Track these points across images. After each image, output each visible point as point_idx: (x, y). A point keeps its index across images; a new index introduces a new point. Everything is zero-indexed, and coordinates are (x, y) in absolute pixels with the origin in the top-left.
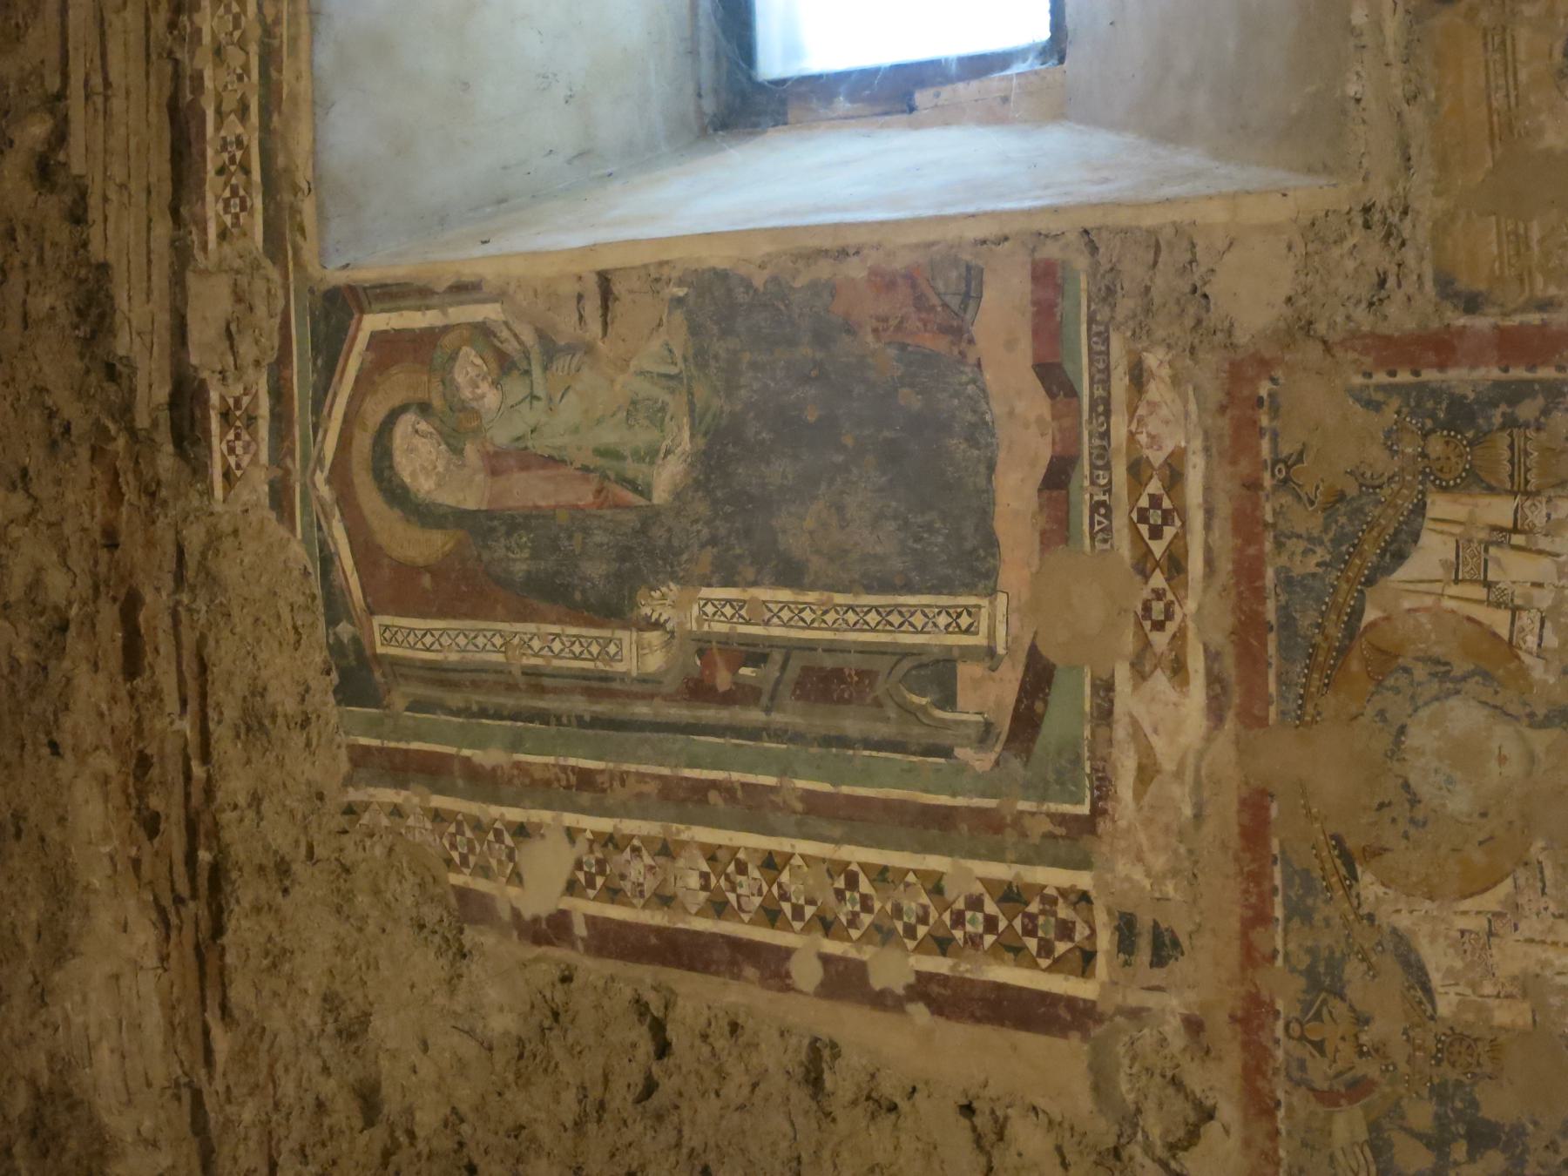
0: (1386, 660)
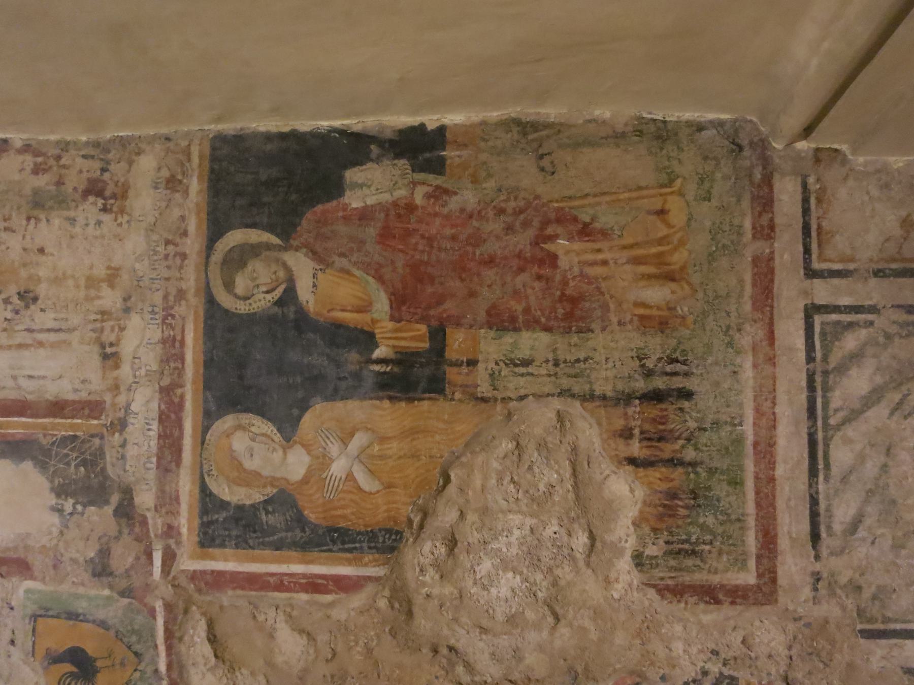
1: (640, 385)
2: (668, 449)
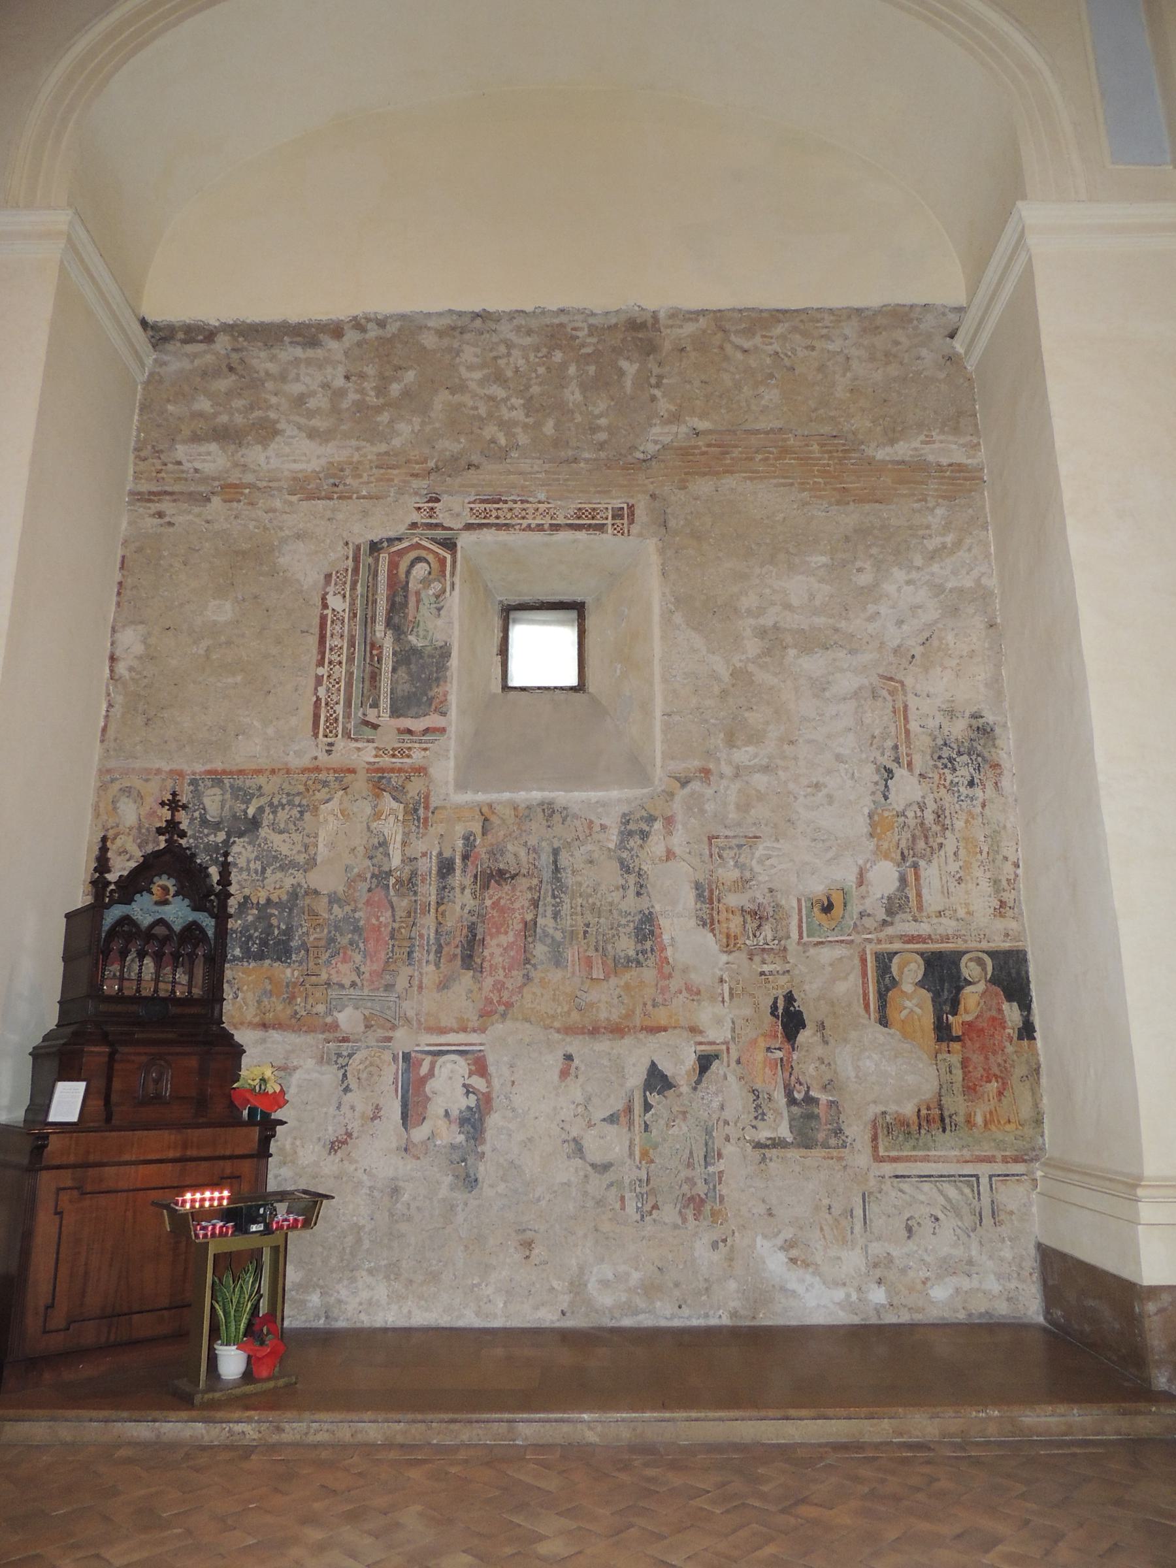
0: (377, 796)
1: (946, 1114)
2: (924, 1124)
